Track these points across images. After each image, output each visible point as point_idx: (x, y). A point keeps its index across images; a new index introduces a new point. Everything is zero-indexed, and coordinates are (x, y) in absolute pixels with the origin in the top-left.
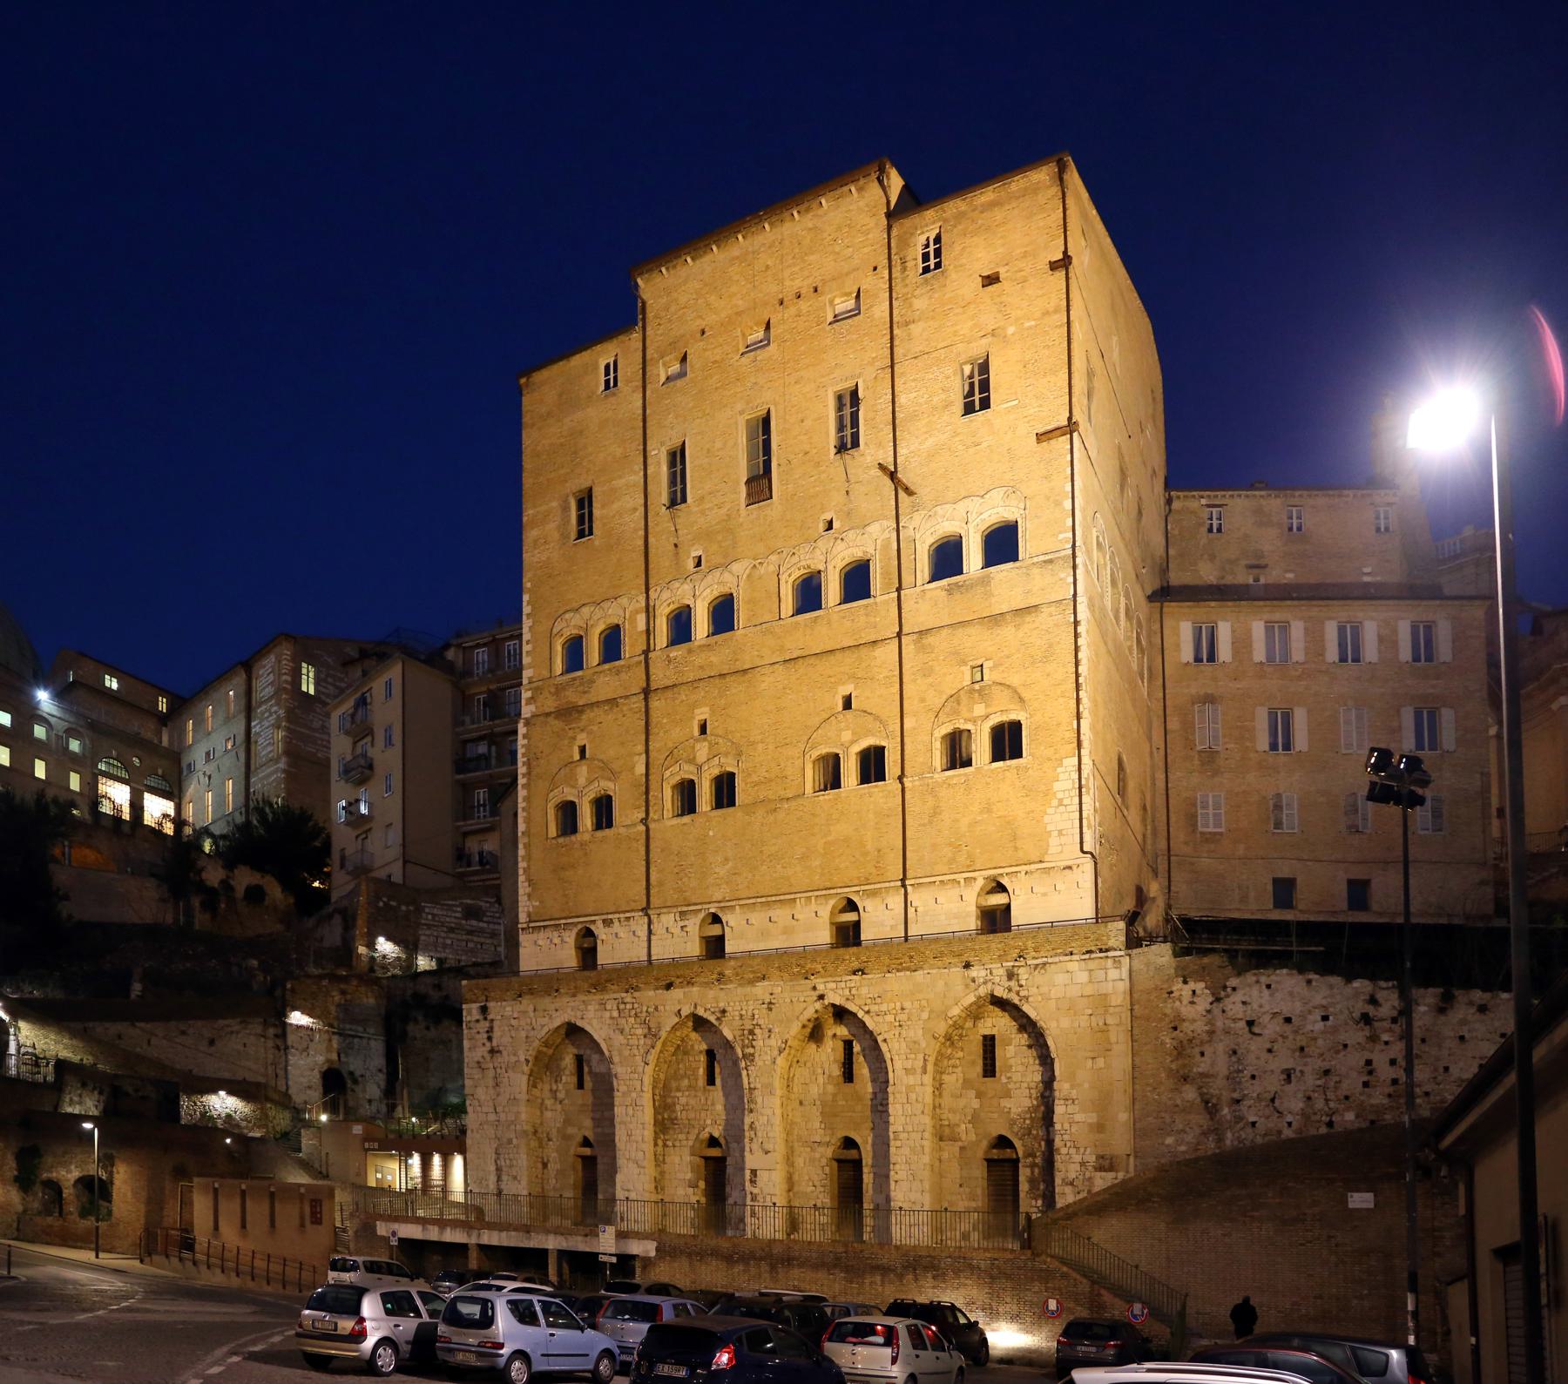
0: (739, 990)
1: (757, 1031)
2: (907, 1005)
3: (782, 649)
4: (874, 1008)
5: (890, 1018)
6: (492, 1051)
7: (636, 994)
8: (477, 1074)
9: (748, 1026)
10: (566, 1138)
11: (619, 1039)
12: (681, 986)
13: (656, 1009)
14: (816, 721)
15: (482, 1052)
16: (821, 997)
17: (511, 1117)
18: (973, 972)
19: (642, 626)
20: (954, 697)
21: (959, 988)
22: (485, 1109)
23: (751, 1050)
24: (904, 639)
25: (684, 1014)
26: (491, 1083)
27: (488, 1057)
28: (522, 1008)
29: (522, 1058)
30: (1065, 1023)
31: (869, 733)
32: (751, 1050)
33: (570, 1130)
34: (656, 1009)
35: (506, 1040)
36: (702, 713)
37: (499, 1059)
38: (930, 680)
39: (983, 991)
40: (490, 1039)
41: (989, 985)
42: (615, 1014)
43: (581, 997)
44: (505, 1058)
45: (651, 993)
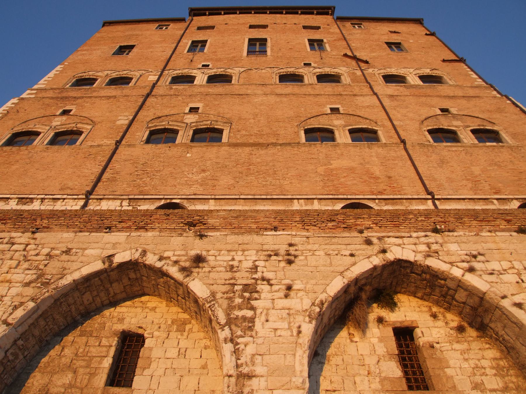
0: (232, 238)
1: (263, 287)
4: (477, 265)
7: (37, 235)
9: (243, 278)
14: (309, 116)
16: (384, 251)
23: (249, 313)
25: (118, 259)
32: (249, 313)
38: (408, 110)
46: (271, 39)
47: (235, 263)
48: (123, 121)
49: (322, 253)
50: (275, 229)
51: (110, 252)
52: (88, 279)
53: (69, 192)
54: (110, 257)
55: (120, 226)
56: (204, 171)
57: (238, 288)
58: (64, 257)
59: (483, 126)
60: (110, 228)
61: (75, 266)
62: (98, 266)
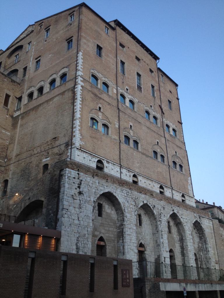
6: (80, 193)
8: (70, 199)
10: (94, 236)
11: (127, 204)
15: (74, 191)
17: (86, 224)
22: (73, 217)
25: (145, 202)
26: (77, 206)
27: (77, 194)
28: (94, 180)
29: (92, 200)
33: (97, 233)
35: (85, 190)
37: (81, 197)
40: (79, 187)
42: (126, 195)
43: (115, 185)
44: (85, 197)
45: (136, 193)
48: (117, 126)
53: (115, 161)
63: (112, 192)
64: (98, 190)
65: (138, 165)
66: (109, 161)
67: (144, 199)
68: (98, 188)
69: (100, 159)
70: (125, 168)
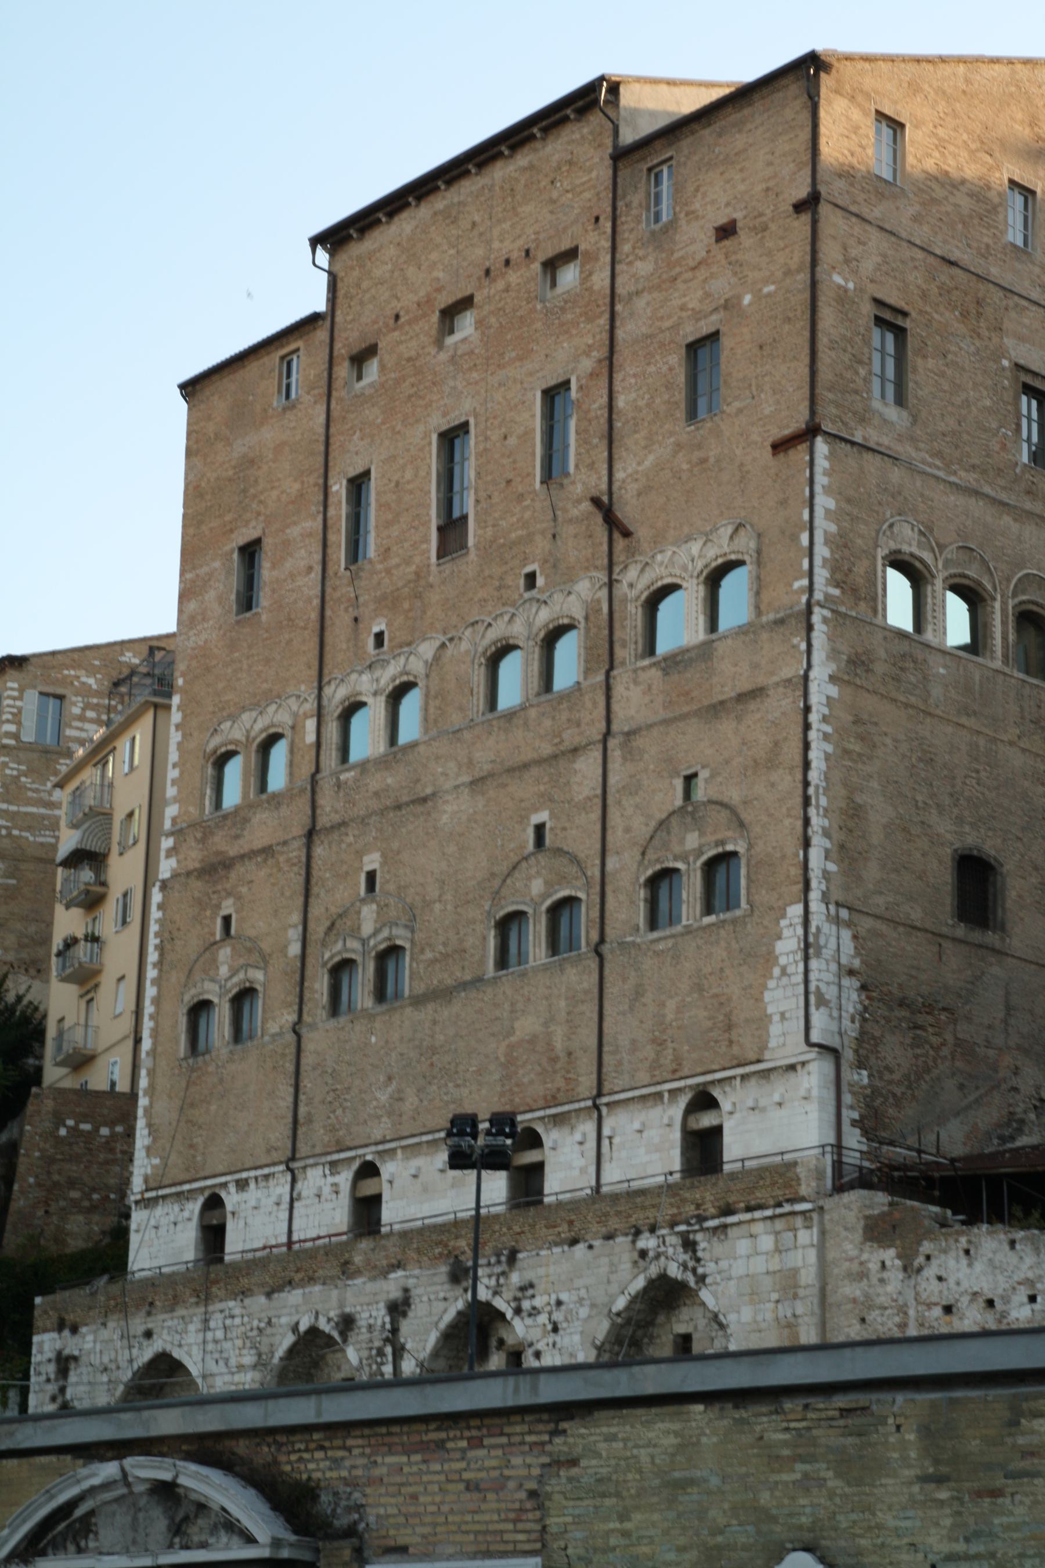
0: (370, 1287)
2: (564, 1297)
3: (470, 763)
4: (526, 1305)
5: (543, 1318)
7: (247, 1301)
12: (301, 1284)
13: (269, 1323)
14: (504, 867)
18: (641, 1244)
19: (311, 738)
20: (663, 824)
21: (626, 1266)
24: (612, 743)
25: (303, 1328)
28: (105, 1334)
30: (747, 1314)
31: (563, 879)
34: (269, 1323)
36: (372, 861)
38: (637, 799)
39: (654, 1271)
40: (62, 1390)
41: (663, 1259)
42: (219, 1334)
43: (181, 1312)
46: (476, 416)
47: (372, 1321)
48: (295, 949)
49: (425, 1299)
50: (399, 1265)
51: (295, 1319)
52: (292, 1351)
54: (295, 1329)
55: (298, 1277)
56: (390, 1079)
57: (374, 1352)
58: (269, 1331)
59: (722, 842)
60: (290, 1283)
61: (278, 1338)
62: (289, 1339)
63: (168, 1348)
64: (118, 1368)
65: (383, 1097)
66: (244, 1175)
67: (297, 1312)
68: (120, 1358)
69: (207, 1194)
70: (311, 1161)
